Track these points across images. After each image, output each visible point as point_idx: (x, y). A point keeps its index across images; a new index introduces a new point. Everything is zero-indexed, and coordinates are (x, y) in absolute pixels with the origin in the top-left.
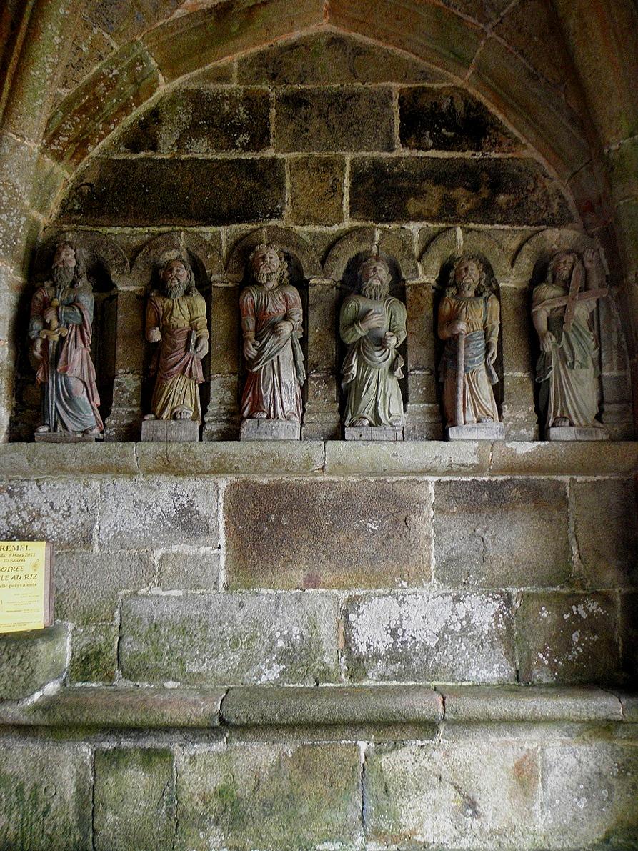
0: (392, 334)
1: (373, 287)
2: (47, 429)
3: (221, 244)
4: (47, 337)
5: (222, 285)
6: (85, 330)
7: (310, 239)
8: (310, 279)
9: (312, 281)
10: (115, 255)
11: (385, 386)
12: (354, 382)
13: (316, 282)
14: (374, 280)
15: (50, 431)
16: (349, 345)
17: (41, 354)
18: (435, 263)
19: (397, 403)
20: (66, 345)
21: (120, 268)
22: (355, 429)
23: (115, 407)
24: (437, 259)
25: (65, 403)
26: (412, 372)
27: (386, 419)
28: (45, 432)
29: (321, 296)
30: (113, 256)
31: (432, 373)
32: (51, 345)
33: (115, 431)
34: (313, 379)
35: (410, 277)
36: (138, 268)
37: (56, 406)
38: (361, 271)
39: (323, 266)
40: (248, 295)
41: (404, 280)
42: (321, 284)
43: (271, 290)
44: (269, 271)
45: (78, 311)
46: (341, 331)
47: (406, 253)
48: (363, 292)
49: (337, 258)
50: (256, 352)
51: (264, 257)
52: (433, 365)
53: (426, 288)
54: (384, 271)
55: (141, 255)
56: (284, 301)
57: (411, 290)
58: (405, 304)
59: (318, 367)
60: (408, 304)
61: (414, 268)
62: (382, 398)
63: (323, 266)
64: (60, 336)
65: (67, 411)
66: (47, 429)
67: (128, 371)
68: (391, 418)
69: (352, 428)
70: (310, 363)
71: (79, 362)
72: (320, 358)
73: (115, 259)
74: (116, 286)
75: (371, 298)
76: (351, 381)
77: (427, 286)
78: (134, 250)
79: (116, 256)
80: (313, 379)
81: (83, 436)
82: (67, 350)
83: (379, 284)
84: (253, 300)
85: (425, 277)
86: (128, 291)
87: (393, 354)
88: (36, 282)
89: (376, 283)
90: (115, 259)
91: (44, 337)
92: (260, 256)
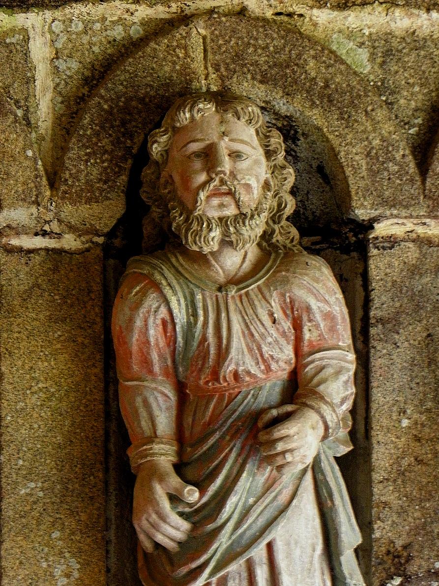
3: (30, 81)
5: (39, 242)
7: (372, 58)
9: (382, 229)
39: (423, 167)
40: (152, 301)
43: (238, 281)
44: (231, 211)
50: (185, 525)
51: (209, 156)
56: (287, 325)
59: (412, 568)
63: (423, 167)
70: (379, 550)
72: (417, 530)
84: (169, 324)
92: (195, 147)
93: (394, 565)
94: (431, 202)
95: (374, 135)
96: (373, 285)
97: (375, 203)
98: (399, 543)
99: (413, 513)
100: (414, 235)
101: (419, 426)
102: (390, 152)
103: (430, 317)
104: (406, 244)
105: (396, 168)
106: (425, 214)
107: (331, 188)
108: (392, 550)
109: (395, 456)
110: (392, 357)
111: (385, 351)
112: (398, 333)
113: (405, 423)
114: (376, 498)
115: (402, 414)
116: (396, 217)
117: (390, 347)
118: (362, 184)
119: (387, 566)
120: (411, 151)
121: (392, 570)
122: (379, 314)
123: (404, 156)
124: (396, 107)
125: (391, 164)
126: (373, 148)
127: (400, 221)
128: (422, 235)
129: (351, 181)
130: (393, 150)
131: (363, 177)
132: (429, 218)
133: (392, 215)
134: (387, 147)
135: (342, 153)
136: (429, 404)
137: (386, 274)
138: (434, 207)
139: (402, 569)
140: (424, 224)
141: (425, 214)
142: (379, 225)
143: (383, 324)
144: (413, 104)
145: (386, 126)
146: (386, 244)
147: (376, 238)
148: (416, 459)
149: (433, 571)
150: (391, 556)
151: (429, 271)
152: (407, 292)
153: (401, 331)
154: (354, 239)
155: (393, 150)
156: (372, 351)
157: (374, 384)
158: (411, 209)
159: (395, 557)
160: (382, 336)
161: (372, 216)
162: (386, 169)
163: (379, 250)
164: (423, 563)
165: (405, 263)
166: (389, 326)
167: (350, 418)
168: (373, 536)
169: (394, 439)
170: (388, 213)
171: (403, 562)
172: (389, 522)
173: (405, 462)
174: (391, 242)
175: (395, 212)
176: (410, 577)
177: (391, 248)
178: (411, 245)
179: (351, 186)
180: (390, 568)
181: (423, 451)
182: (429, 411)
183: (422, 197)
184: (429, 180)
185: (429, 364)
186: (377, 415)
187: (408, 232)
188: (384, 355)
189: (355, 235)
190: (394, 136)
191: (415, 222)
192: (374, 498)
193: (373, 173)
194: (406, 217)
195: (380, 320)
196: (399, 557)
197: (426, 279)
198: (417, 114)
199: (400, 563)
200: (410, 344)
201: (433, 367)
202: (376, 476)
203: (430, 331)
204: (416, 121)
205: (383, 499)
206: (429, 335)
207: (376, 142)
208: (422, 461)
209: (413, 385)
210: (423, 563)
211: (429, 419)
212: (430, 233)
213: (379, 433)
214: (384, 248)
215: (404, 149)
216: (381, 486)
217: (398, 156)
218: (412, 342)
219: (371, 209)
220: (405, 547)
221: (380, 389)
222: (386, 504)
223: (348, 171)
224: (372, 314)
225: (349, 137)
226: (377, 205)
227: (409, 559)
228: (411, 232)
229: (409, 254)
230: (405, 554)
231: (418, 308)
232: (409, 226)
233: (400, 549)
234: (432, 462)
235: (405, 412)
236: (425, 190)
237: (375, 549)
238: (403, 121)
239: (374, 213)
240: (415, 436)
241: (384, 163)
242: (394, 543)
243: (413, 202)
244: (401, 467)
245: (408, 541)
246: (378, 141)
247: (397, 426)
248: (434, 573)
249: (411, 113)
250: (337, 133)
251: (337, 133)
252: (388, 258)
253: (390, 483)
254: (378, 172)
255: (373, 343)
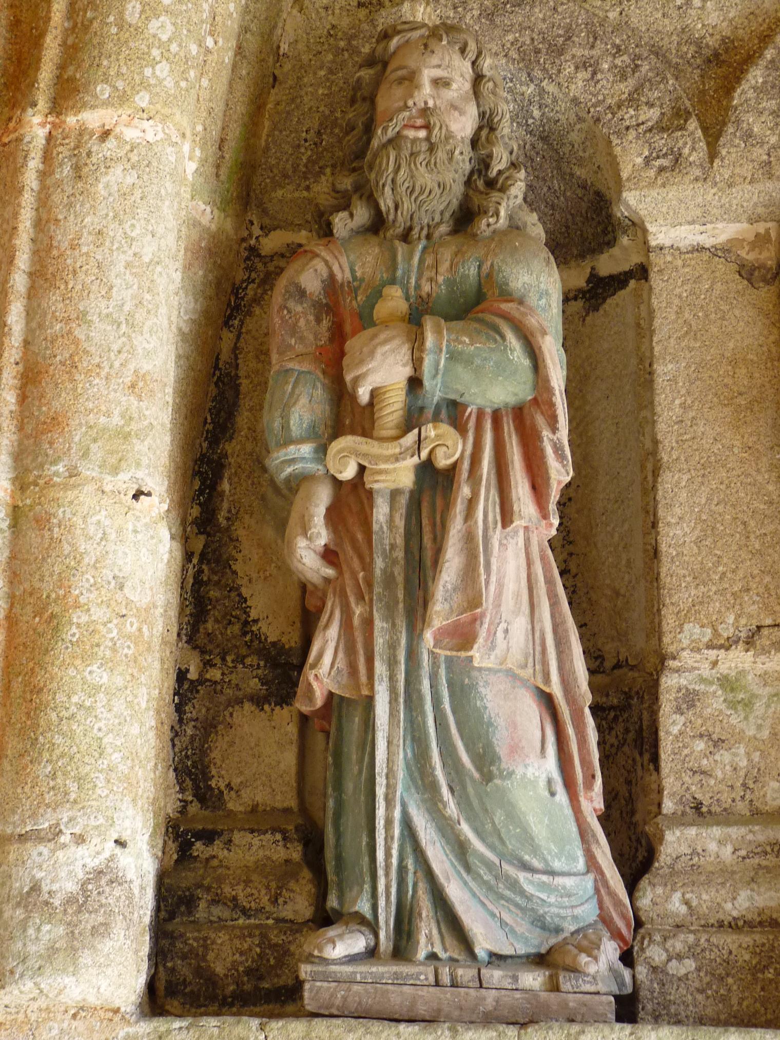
2: (358, 943)
4: (362, 469)
6: (546, 433)
10: (631, 83)
15: (372, 953)
17: (329, 555)
20: (459, 508)
21: (661, 141)
23: (679, 820)
25: (452, 809)
28: (352, 959)
30: (625, 88)
32: (381, 512)
33: (692, 952)
36: (748, 135)
37: (407, 824)
45: (511, 337)
55: (756, 76)
64: (426, 469)
65: (461, 849)
66: (358, 943)
67: (726, 631)
71: (517, 595)
73: (632, 100)
74: (637, 227)
78: (715, 59)
79: (639, 89)
81: (554, 987)
82: (469, 538)
86: (700, 249)
88: (266, 230)
90: (632, 100)
91: (349, 473)
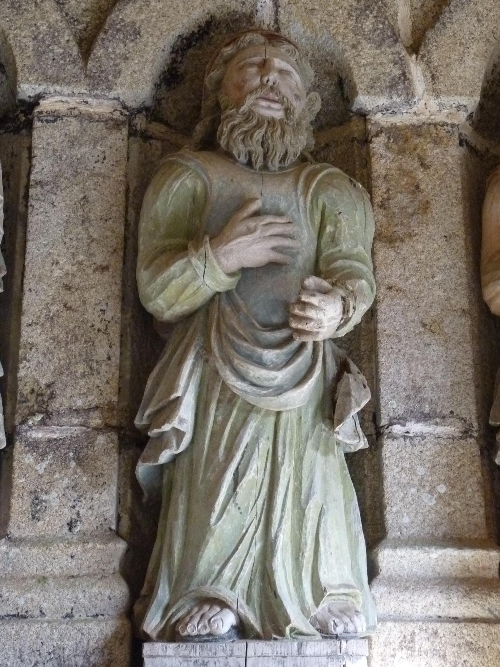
0: (325, 284)
1: (258, 126)
8: (39, 97)
9: (46, 105)
11: (299, 479)
12: (184, 464)
13: (62, 108)
14: (264, 103)
16: (169, 326)
18: (469, 61)
19: (346, 548)
22: (183, 648)
24: (474, 48)
26: (397, 429)
27: (304, 611)
29: (78, 152)
31: (466, 433)
34: (34, 446)
35: (383, 101)
38: (214, 74)
41: (363, 115)
42: (80, 116)
46: (143, 275)
47: (368, 25)
48: (223, 143)
49: (137, 33)
52: (473, 408)
53: (437, 141)
54: (297, 77)
57: (388, 147)
58: (370, 190)
59: (54, 406)
60: (380, 193)
61: (397, 72)
62: (287, 526)
68: (324, 604)
69: (171, 647)
70: (24, 389)
75: (250, 164)
76: (175, 459)
77: (442, 133)
80: (34, 446)
83: (279, 115)
85: (433, 104)
87: (330, 360)
89: (268, 113)
93: (37, 403)
94: (92, 81)
95: (42, 22)
96: (35, 152)
97: (40, 79)
98: (43, 382)
99: (58, 354)
100: (76, 112)
101: (70, 276)
102: (56, 37)
103: (86, 181)
104: (69, 119)
105: (61, 51)
106: (86, 91)
107: (7, 77)
108: (36, 389)
109: (44, 303)
110: (48, 215)
111: (42, 210)
112: (56, 194)
113: (57, 273)
114: (23, 340)
115: (54, 265)
116: (60, 94)
117: (47, 206)
118: (28, 62)
119: (30, 404)
120: (77, 43)
121: (35, 407)
122: (39, 178)
123: (68, 41)
124: (67, 6)
125: (56, 47)
126: (40, 33)
127: (64, 99)
128: (84, 112)
129: (18, 60)
130: (58, 35)
131: (29, 57)
132: (90, 97)
133: (55, 91)
134: (54, 33)
135: (11, 36)
136: (81, 257)
137: (48, 144)
138: (93, 86)
139: (45, 406)
140: (86, 102)
141: (86, 91)
142: (44, 102)
143: (42, 187)
144: (83, 5)
145: (54, 16)
146: (49, 118)
147: (41, 112)
148: (65, 306)
149: (74, 408)
150: (35, 395)
151: (88, 143)
152: (66, 159)
153: (58, 193)
154: (24, 118)
155: (58, 35)
156: (30, 209)
157: (30, 237)
158: (73, 86)
159: (38, 395)
160: (40, 196)
161: (38, 92)
162: (52, 51)
163: (42, 122)
164: (65, 401)
165: (66, 135)
166: (48, 188)
167: (5, 268)
168: (19, 375)
169: (45, 287)
170: (51, 89)
171: (45, 399)
172: (35, 362)
173: (54, 308)
174: (54, 116)
175: (58, 88)
176: (51, 414)
177: (53, 122)
178: (73, 120)
179: (18, 64)
180: (33, 406)
181: (72, 299)
182: (80, 263)
183: (83, 76)
184: (90, 62)
185: (83, 221)
186: (30, 265)
187: (71, 108)
188: (41, 213)
189: (26, 115)
190: (60, 24)
191: (78, 101)
192: (22, 340)
193: (39, 54)
194: (69, 95)
195: (40, 183)
196: (42, 395)
197: (85, 149)
198: (87, 13)
199: (43, 401)
200: (66, 204)
201: (87, 224)
202: (25, 320)
203: (86, 194)
204: (84, 19)
205: (30, 340)
206: (84, 198)
207: (44, 28)
208: (71, 307)
209: (67, 240)
210: (65, 401)
211: (79, 270)
212: (91, 110)
213: (31, 281)
214: (47, 121)
215: (69, 35)
216: (29, 329)
217: (63, 41)
218: (68, 202)
219: (35, 84)
220: (48, 386)
221: (35, 242)
222: (32, 345)
223: (16, 52)
224: (32, 177)
225: (19, 23)
226: (41, 81)
227: (52, 396)
228: (74, 108)
229: (71, 127)
230: (48, 392)
231: (76, 173)
232: (73, 102)
233: (43, 387)
234: (80, 309)
235: (57, 263)
236: (86, 70)
237: (20, 387)
238: (72, 18)
239: (39, 89)
240: (66, 285)
241: (49, 45)
242: (37, 381)
243: (75, 80)
244: (50, 312)
245: (51, 380)
246: (45, 28)
247: (49, 275)
248: (75, 410)
249: (80, 12)
250: (7, 19)
251: (7, 19)
252: (50, 130)
253: (38, 326)
254: (44, 52)
255: (32, 202)
